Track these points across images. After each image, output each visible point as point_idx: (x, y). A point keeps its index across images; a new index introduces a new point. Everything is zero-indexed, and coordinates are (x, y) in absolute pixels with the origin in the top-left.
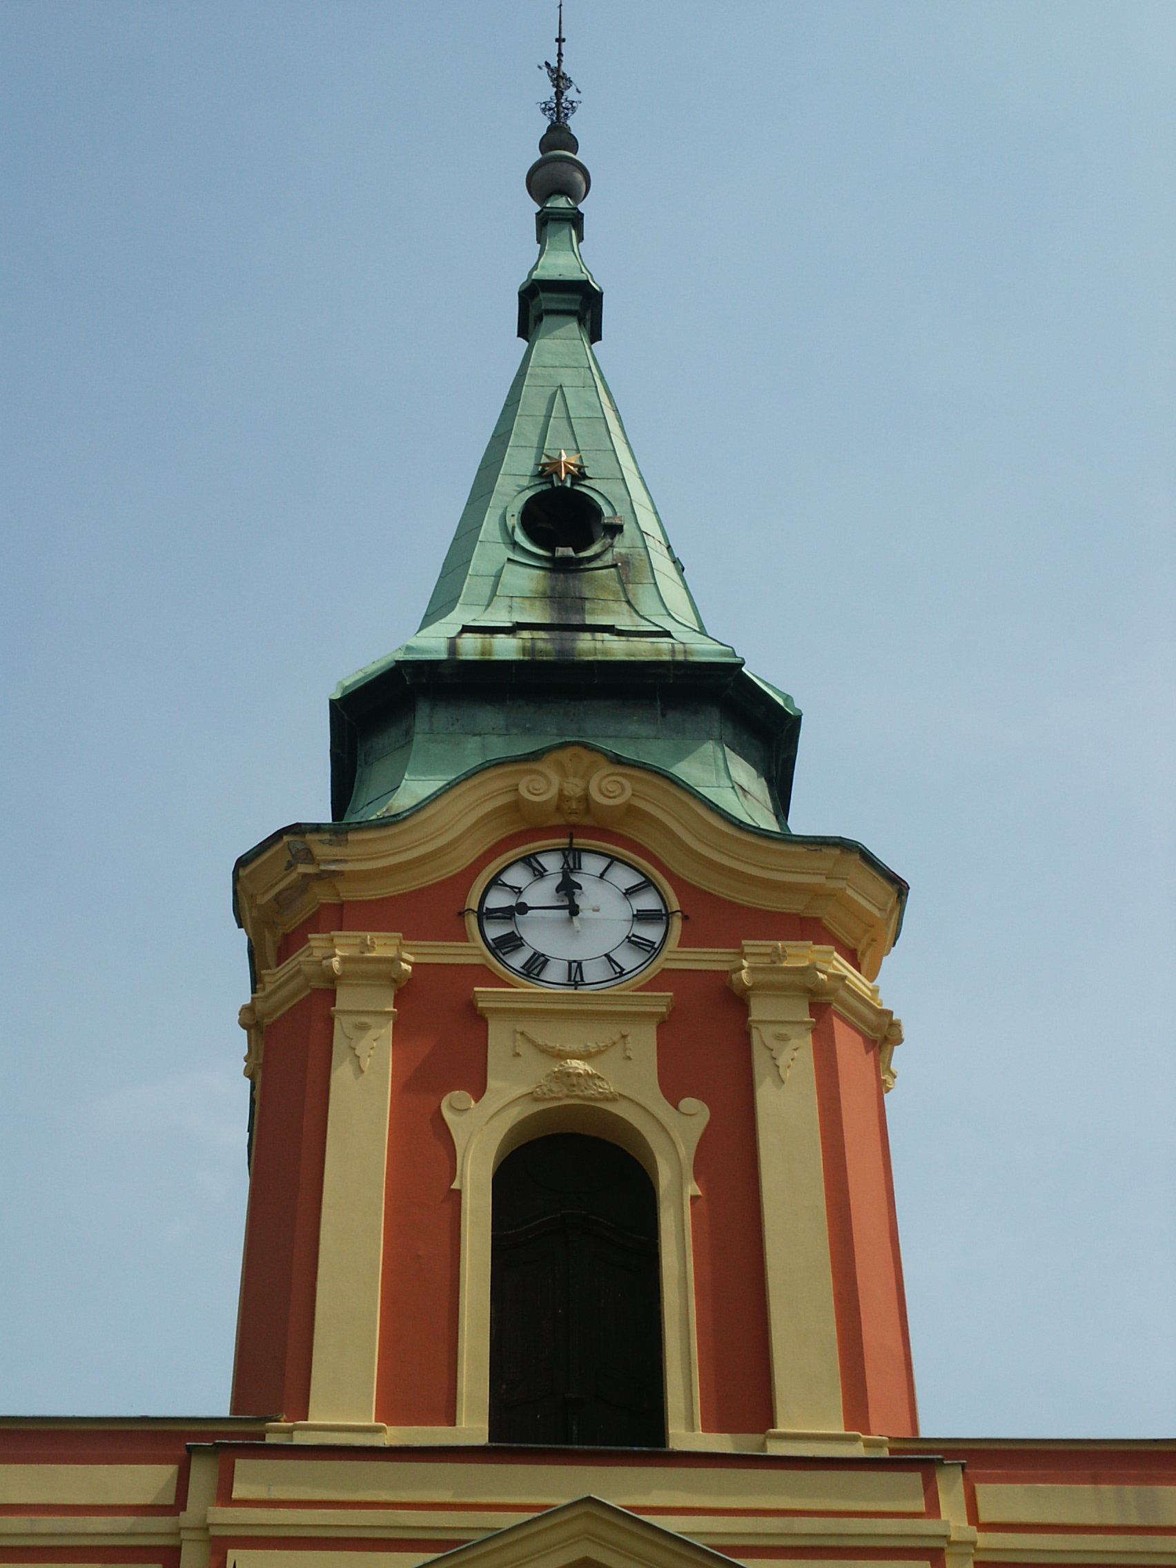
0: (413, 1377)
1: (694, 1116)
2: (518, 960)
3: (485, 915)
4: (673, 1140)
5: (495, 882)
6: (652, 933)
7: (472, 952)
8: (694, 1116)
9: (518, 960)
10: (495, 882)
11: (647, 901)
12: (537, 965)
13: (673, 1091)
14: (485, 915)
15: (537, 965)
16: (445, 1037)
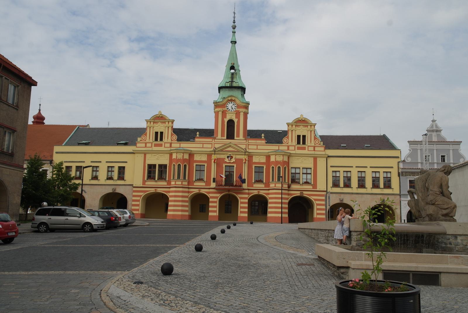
0: (222, 135)
1: (237, 119)
2: (228, 110)
3: (227, 107)
4: (236, 121)
5: (227, 104)
6: (235, 108)
7: (226, 109)
8: (237, 119)
9: (228, 110)
10: (227, 104)
11: (235, 106)
12: (229, 110)
13: (236, 118)
14: (227, 107)
15: (229, 110)
16: (224, 114)
